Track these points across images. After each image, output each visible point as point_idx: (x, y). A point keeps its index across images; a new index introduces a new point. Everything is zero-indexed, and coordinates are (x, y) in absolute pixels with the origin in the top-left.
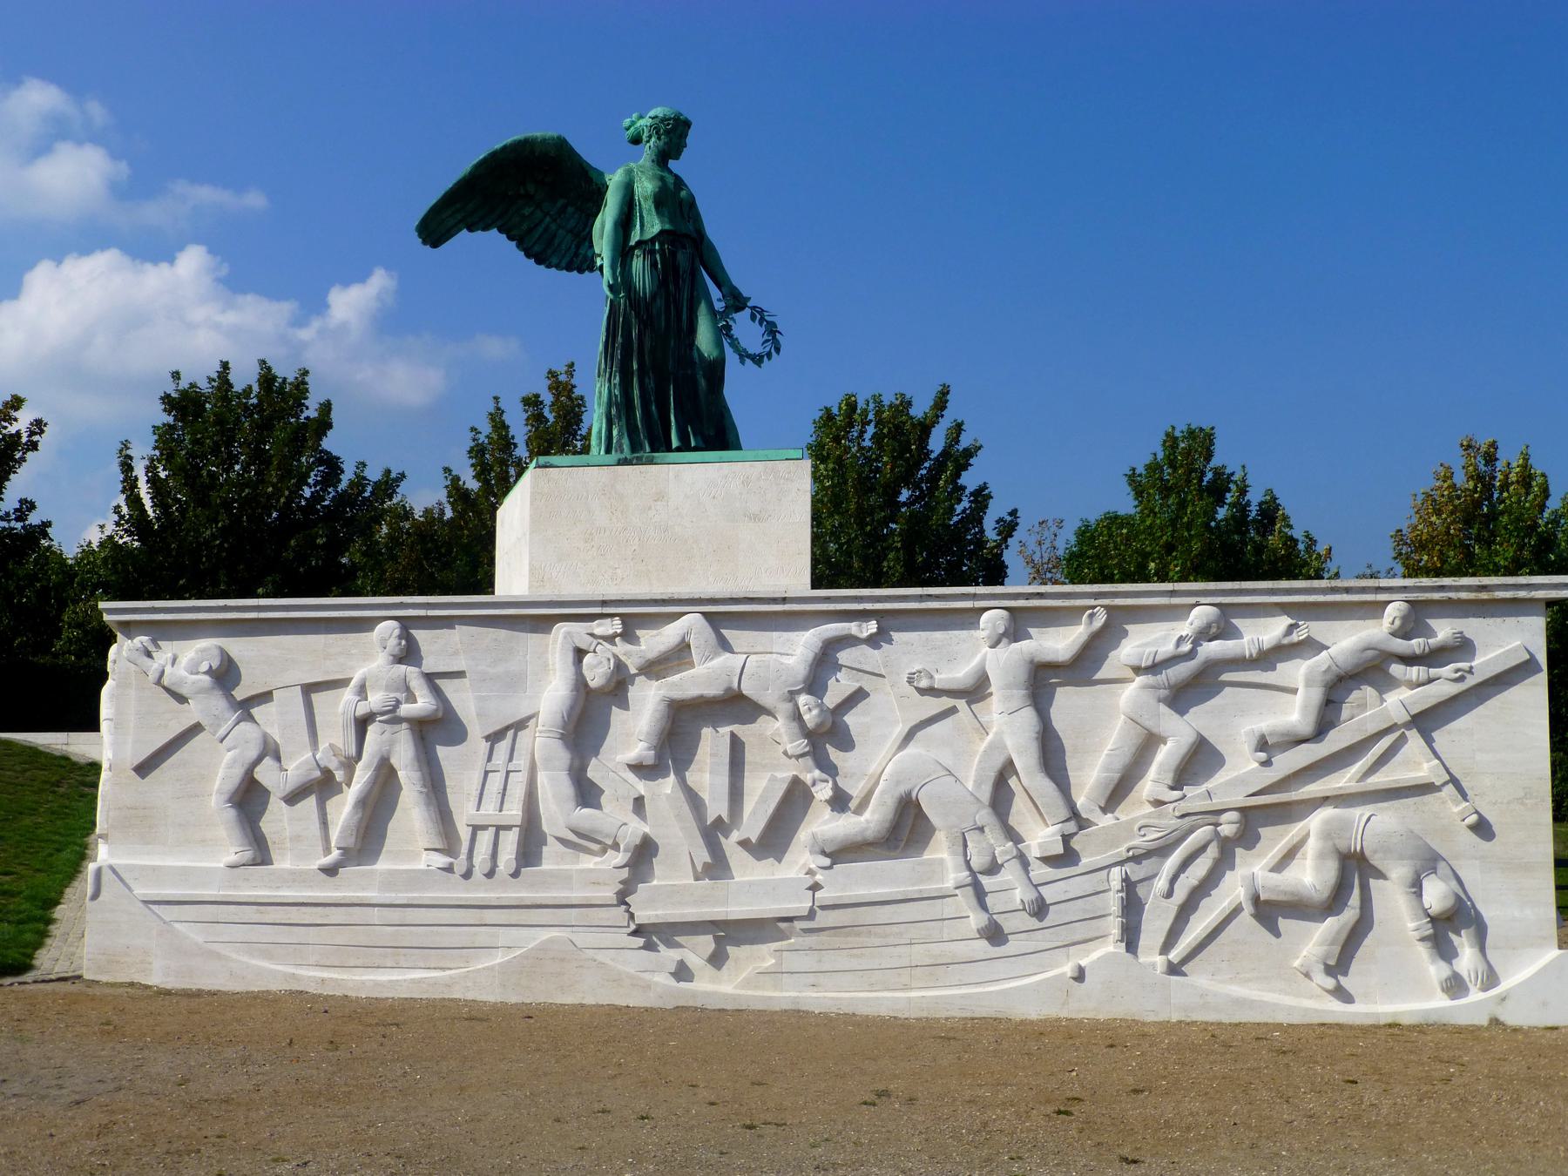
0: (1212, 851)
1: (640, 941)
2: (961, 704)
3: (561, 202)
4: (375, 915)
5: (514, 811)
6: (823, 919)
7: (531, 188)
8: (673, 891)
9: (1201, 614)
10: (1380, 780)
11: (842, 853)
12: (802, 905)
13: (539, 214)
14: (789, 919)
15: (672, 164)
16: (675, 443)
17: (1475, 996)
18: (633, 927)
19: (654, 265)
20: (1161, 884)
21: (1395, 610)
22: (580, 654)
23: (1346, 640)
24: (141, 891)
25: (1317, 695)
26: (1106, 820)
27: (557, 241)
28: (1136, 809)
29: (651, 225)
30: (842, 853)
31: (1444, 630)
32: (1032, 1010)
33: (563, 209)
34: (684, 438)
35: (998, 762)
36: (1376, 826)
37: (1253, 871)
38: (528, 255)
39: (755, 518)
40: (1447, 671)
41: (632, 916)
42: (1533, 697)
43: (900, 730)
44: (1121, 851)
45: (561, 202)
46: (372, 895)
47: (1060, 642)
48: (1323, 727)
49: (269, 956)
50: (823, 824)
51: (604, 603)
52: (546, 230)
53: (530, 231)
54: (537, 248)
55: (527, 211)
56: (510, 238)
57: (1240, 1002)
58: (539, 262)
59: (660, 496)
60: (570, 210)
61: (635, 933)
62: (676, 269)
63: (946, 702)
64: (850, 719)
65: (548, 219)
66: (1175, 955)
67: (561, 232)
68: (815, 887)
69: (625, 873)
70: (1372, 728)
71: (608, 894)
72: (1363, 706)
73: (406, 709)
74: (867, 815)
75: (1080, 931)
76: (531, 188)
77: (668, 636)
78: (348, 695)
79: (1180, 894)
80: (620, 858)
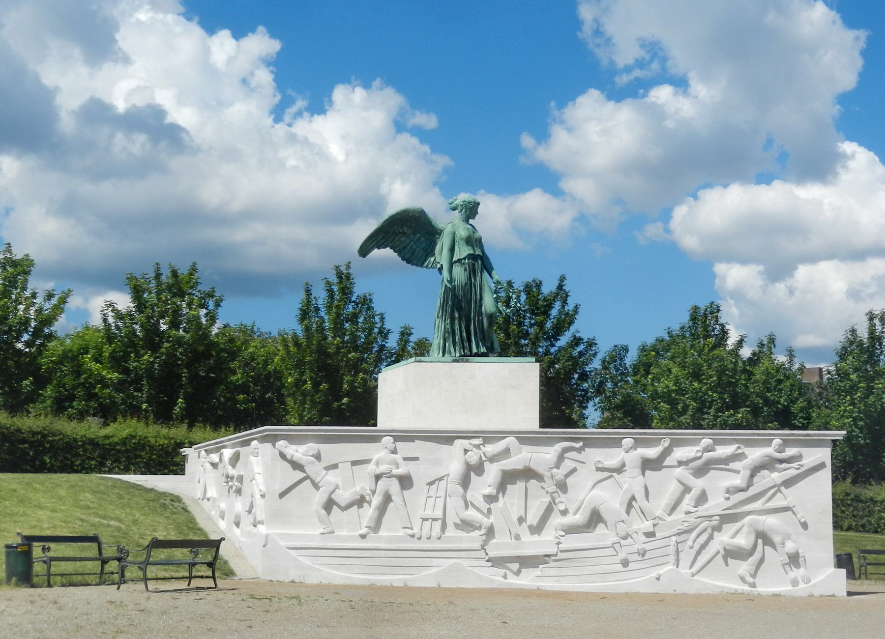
0: (709, 530)
1: (490, 564)
2: (615, 474)
3: (418, 235)
4: (383, 553)
5: (439, 513)
6: (561, 556)
7: (405, 229)
8: (501, 546)
9: (706, 441)
10: (771, 505)
11: (571, 530)
12: (552, 550)
13: (408, 241)
14: (548, 556)
15: (471, 221)
16: (475, 350)
17: (802, 585)
18: (487, 558)
19: (465, 270)
20: (690, 543)
21: (777, 441)
22: (466, 451)
23: (755, 454)
24: (283, 544)
25: (747, 473)
26: (669, 519)
27: (416, 254)
28: (679, 515)
29: (463, 251)
30: (571, 530)
31: (791, 451)
32: (642, 590)
33: (419, 239)
34: (478, 347)
35: (629, 496)
36: (770, 522)
37: (724, 538)
38: (403, 259)
40: (795, 465)
41: (487, 554)
42: (826, 475)
43: (591, 483)
44: (675, 530)
45: (418, 235)
46: (382, 545)
47: (652, 452)
48: (750, 484)
50: (557, 520)
51: (476, 432)
52: (411, 248)
53: (404, 248)
54: (407, 256)
55: (403, 239)
56: (395, 251)
57: (718, 586)
58: (408, 262)
60: (422, 239)
61: (488, 561)
63: (606, 474)
64: (569, 481)
65: (412, 243)
66: (694, 570)
67: (418, 249)
68: (558, 543)
69: (484, 537)
70: (767, 486)
71: (477, 545)
72: (764, 477)
73: (395, 472)
74: (577, 516)
75: (660, 560)
76: (405, 229)
77: (500, 445)
78: (371, 468)
79: (697, 546)
80: (483, 531)
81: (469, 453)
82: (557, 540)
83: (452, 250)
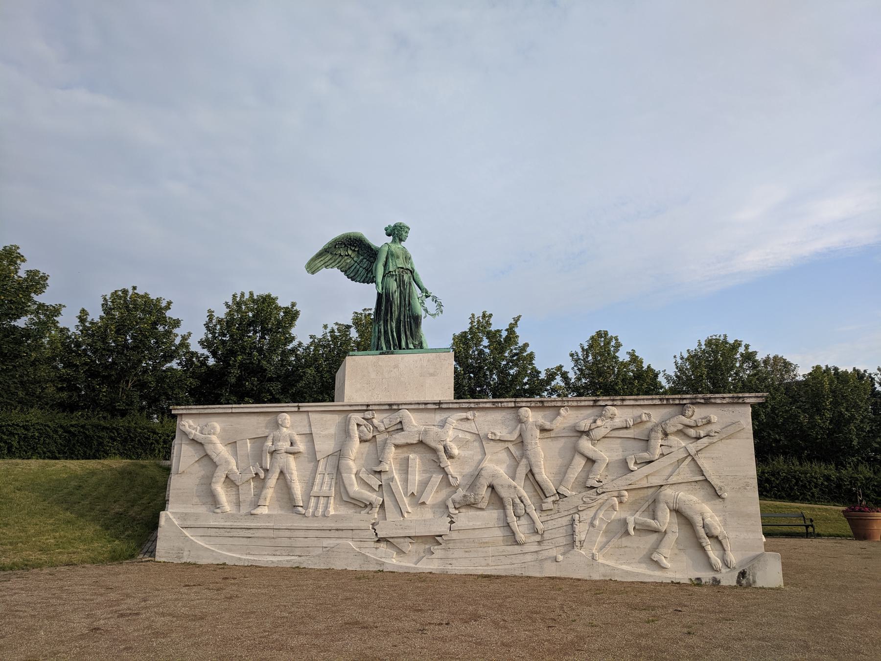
6: (454, 535)
22: (358, 425)
33: (361, 261)
34: (407, 344)
39: (431, 375)
46: (271, 525)
49: (230, 550)
58: (352, 280)
59: (396, 366)
62: (404, 281)
76: (350, 252)
81: (363, 428)
82: (449, 519)
83: (386, 265)
